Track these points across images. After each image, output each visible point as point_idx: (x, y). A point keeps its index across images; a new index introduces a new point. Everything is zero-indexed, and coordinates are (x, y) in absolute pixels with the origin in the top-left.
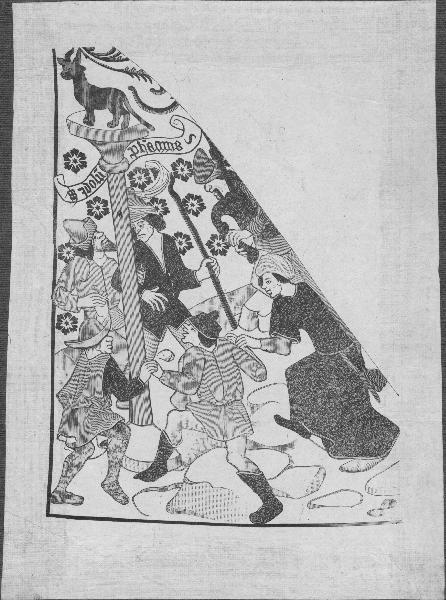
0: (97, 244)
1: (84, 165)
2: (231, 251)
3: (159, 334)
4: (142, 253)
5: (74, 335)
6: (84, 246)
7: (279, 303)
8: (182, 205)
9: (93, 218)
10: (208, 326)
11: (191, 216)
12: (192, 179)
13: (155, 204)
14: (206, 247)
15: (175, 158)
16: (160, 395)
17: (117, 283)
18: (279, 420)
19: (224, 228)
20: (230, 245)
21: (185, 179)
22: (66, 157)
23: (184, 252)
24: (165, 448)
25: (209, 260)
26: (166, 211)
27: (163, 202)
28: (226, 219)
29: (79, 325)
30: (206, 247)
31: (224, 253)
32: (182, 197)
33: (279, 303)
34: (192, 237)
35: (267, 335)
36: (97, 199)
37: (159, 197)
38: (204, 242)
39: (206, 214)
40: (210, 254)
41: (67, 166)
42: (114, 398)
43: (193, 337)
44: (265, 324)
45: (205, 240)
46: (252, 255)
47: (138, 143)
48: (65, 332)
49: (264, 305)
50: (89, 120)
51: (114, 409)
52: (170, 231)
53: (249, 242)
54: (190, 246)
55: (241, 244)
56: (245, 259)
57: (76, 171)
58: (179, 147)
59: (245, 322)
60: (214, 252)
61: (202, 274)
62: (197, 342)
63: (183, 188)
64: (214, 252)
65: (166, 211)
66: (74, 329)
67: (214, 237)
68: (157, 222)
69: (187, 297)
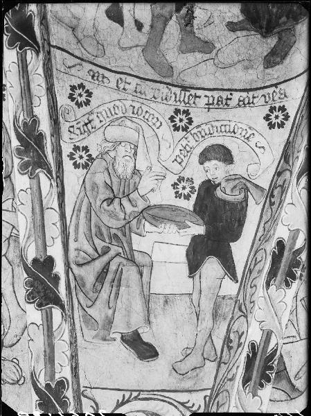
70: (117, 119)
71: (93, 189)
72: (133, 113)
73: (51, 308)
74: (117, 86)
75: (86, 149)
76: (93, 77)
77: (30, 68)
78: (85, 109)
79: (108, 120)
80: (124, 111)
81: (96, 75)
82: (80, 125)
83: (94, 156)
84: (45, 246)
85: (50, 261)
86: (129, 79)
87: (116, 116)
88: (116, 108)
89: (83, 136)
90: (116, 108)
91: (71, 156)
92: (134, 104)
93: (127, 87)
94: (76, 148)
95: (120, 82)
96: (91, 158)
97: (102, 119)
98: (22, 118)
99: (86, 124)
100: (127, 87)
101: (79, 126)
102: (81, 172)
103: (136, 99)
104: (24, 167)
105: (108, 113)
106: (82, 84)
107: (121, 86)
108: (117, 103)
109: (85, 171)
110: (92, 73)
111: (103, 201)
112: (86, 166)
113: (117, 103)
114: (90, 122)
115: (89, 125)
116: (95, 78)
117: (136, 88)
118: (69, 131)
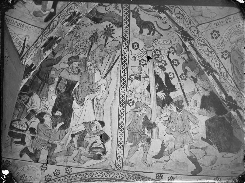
0: (142, 75)
1: (138, 48)
2: (188, 79)
5: (133, 107)
6: (137, 75)
7: (204, 98)
9: (141, 66)
10: (180, 107)
11: (174, 66)
12: (175, 54)
13: (163, 62)
15: (169, 46)
16: (162, 128)
17: (148, 89)
18: (202, 138)
19: (186, 71)
20: (188, 77)
21: (173, 53)
22: (133, 44)
23: (172, 79)
24: (163, 147)
25: (180, 82)
26: (166, 65)
28: (187, 68)
29: (135, 103)
30: (180, 78)
31: (185, 80)
32: (172, 60)
34: (175, 74)
35: (199, 109)
36: (143, 59)
37: (164, 60)
38: (179, 76)
39: (180, 66)
40: (181, 80)
41: (133, 48)
42: (146, 129)
43: (174, 108)
44: (199, 105)
46: (195, 81)
47: (157, 41)
48: (130, 106)
50: (141, 32)
51: (146, 133)
52: (167, 71)
54: (174, 77)
55: (192, 77)
57: (136, 49)
60: (182, 79)
61: (178, 87)
62: (175, 110)
64: (182, 79)
65: (166, 65)
66: (133, 104)
67: (182, 74)
68: (163, 68)
69: (172, 95)
70: (232, 34)
71: (235, 62)
72: (237, 28)
74: (227, 22)
75: (226, 51)
76: (216, 25)
77: (194, 45)
78: (219, 38)
79: (229, 36)
80: (233, 29)
81: (217, 23)
82: (220, 44)
83: (230, 52)
85: (231, 97)
86: (229, 17)
87: (231, 33)
88: (230, 30)
89: (223, 48)
90: (230, 30)
91: (222, 57)
92: (236, 25)
93: (230, 20)
94: (223, 53)
95: (227, 20)
96: (229, 53)
97: (227, 37)
99: (222, 43)
100: (230, 20)
101: (220, 45)
102: (229, 59)
103: (235, 22)
104: (208, 73)
105: (228, 33)
106: (214, 30)
107: (228, 21)
108: (230, 28)
109: (229, 58)
110: (215, 24)
111: (241, 65)
112: (229, 57)
113: (230, 28)
114: (223, 41)
115: (223, 43)
116: (218, 25)
117: (234, 18)
118: (218, 49)
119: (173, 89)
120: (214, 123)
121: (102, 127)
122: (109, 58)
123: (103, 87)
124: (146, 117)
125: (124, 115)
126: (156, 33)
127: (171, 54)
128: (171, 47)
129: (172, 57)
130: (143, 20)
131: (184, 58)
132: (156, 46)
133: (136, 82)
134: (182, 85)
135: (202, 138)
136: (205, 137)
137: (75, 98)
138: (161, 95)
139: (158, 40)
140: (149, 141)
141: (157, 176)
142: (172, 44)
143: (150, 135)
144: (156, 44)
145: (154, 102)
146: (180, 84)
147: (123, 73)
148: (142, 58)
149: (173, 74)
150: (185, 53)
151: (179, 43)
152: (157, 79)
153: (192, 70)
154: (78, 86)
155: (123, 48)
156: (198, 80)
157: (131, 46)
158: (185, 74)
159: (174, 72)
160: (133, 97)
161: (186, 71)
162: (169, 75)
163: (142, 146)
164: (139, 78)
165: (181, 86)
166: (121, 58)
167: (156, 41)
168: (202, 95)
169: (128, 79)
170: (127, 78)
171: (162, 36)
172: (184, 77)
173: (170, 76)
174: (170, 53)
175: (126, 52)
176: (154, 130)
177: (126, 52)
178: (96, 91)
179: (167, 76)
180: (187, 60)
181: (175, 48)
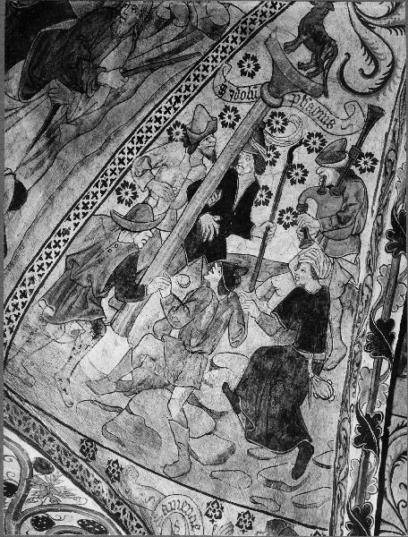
0: (204, 143)
1: (252, 75)
2: (293, 229)
3: (192, 257)
4: (230, 179)
5: (123, 210)
7: (299, 293)
8: (290, 165)
10: (230, 279)
11: (288, 181)
12: (314, 155)
13: (270, 152)
14: (277, 213)
16: (150, 311)
17: (192, 190)
19: (303, 208)
21: (310, 151)
23: (258, 204)
27: (277, 155)
29: (135, 202)
30: (277, 213)
31: (286, 226)
32: (295, 161)
33: (299, 293)
35: (269, 312)
36: (235, 110)
40: (276, 221)
41: (240, 64)
42: (112, 292)
43: (215, 276)
44: (276, 300)
45: (283, 205)
46: (305, 239)
47: (305, 96)
48: (120, 200)
49: (285, 286)
50: (290, 48)
51: (105, 302)
52: (263, 181)
53: (312, 232)
54: (266, 203)
56: (298, 243)
57: (243, 73)
58: (331, 124)
59: (261, 290)
60: (280, 221)
61: (257, 232)
62: (214, 285)
63: (301, 156)
64: (280, 221)
65: (273, 163)
66: (129, 203)
67: (290, 209)
68: (260, 167)
69: (234, 243)
73: (382, 359)
84: (390, 311)
85: (392, 323)
98: (400, 208)
119: (245, 230)
120: (271, 363)
121: (11, 209)
122: (180, 36)
123: (99, 98)
124: (132, 261)
125: (85, 214)
126: (319, 79)
127: (303, 148)
128: (319, 135)
129: (301, 156)
130: (326, 26)
131: (325, 178)
132: (290, 104)
133: (177, 151)
134: (269, 233)
135: (225, 385)
136: (233, 386)
137: (29, 57)
138: (209, 223)
139: (308, 97)
140: (97, 330)
141: (83, 447)
142: (329, 130)
143: (109, 313)
144: (293, 102)
145: (181, 230)
146: (268, 229)
147: (170, 100)
148: (235, 105)
149: (270, 194)
150: (339, 170)
151: (348, 138)
152: (230, 179)
153: (319, 217)
154: (63, 32)
155: (221, 44)
156: (315, 245)
157: (240, 56)
158: (296, 215)
159: (274, 192)
160: (141, 183)
161: (303, 208)
162: (260, 192)
163: (76, 334)
164: (191, 144)
165: (266, 235)
166: (198, 63)
167: (302, 95)
168: (298, 283)
169: (168, 128)
170: (168, 124)
171: (327, 96)
172: (288, 218)
173: (260, 196)
174: (303, 146)
175: (219, 60)
176: (132, 306)
177: (219, 60)
178: (82, 92)
179: (254, 187)
180: (328, 187)
181: (327, 144)
